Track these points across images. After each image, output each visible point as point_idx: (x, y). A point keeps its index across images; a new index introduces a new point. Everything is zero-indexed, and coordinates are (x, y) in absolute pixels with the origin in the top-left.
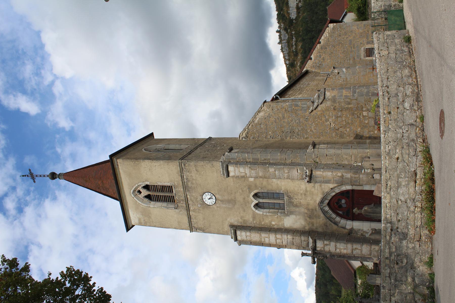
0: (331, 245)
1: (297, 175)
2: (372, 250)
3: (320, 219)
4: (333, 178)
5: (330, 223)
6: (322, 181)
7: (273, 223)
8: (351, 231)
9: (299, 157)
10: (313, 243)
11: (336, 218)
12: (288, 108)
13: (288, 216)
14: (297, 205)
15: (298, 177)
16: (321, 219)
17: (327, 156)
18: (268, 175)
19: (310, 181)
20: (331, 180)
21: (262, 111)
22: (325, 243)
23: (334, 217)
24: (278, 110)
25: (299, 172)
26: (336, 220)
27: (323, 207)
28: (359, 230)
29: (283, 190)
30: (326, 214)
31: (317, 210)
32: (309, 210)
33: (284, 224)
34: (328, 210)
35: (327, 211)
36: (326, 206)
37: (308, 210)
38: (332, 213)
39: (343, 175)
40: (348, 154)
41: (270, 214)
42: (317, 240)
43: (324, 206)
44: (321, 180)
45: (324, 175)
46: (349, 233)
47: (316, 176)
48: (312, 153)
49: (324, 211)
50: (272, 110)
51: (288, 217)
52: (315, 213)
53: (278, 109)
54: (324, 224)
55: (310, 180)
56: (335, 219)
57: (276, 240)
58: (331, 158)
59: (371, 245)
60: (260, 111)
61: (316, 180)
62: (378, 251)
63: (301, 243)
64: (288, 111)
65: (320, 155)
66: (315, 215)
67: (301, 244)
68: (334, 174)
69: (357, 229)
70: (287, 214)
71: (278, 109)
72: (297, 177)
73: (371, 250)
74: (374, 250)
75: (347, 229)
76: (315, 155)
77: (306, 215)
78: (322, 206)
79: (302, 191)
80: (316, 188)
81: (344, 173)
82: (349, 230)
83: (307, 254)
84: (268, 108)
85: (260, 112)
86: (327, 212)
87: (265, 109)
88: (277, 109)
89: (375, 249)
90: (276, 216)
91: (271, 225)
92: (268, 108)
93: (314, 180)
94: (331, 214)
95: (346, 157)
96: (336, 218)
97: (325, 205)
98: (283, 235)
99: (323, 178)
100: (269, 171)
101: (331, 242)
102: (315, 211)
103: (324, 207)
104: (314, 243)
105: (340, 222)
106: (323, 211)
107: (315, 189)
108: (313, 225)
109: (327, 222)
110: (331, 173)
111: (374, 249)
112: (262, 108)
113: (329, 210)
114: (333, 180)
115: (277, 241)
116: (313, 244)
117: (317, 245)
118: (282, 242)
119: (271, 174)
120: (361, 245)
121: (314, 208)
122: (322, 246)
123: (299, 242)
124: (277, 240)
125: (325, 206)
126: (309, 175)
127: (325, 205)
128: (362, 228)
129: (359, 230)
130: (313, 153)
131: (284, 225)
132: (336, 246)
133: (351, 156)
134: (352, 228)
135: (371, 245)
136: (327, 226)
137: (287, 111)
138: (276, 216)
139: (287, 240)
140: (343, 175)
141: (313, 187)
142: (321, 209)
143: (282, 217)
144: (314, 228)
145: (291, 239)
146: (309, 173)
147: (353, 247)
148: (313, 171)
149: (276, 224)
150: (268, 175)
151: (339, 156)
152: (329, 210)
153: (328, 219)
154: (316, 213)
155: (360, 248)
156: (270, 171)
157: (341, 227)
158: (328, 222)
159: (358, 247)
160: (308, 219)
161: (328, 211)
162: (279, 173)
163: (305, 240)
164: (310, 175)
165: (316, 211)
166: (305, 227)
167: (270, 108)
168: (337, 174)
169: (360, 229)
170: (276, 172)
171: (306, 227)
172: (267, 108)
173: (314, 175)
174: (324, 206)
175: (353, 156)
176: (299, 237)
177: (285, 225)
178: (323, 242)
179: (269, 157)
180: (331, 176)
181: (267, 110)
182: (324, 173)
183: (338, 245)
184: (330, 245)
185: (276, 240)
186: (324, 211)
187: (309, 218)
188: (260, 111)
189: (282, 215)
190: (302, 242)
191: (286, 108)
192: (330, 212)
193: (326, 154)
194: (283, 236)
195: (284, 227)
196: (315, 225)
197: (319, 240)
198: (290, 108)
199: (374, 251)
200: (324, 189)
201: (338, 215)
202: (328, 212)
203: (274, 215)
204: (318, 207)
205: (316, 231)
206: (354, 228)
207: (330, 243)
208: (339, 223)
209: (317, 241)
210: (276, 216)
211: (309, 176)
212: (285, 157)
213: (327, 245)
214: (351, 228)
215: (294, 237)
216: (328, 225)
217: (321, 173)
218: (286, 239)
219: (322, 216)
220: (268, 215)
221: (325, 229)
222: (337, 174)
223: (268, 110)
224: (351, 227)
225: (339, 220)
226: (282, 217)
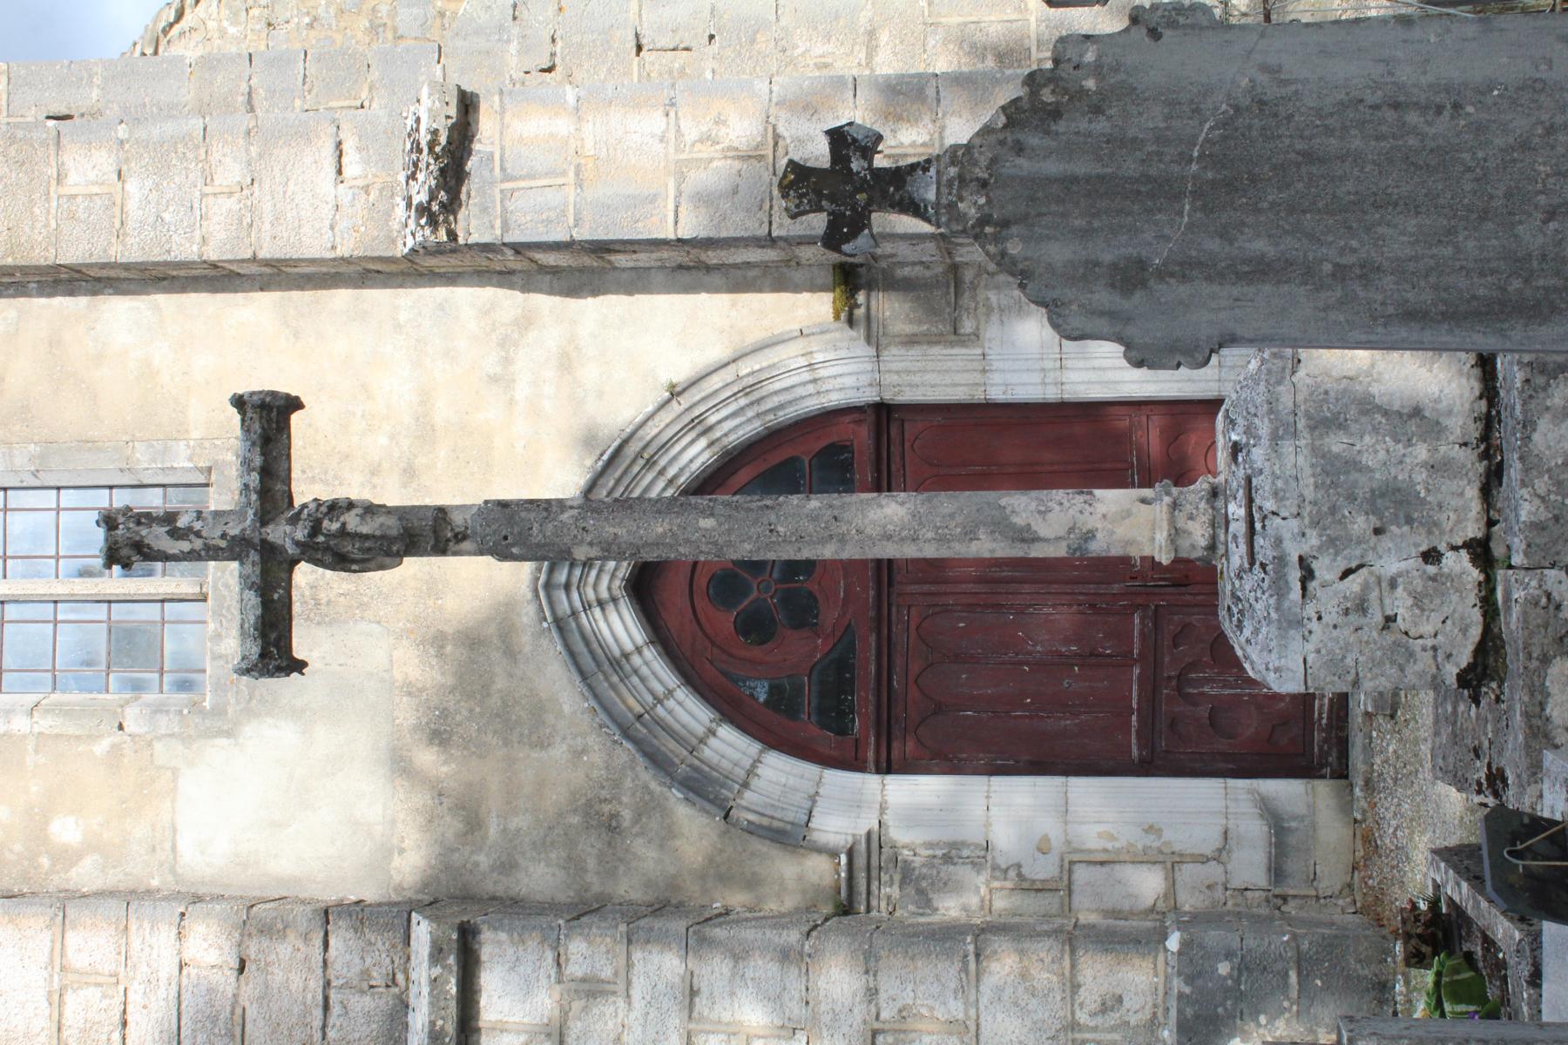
0: (636, 993)
1: (327, 211)
2: (1082, 1017)
3: (543, 744)
4: (681, 178)
5: (646, 787)
6: (564, 213)
7: (66, 831)
8: (861, 877)
9: (375, 74)
10: (437, 954)
11: (713, 733)
12: (393, 13)
13: (229, 734)
14: (318, 604)
15: (342, 225)
16: (559, 752)
17: (639, 48)
18: (47, 225)
19: (442, 205)
20: (653, 199)
21: (182, 34)
22: (579, 974)
23: (693, 725)
24: (311, 26)
25: (352, 167)
26: (707, 753)
27: (587, 607)
28: (947, 859)
29: (195, 434)
30: (613, 687)
31: (525, 640)
32: (440, 655)
33: (175, 831)
34: (629, 647)
35: (626, 656)
36: (614, 600)
37: (438, 641)
38: (669, 678)
39: (777, 138)
40: (837, 18)
41: (45, 723)
42: (486, 935)
43: (591, 595)
44: (553, 198)
45: (589, 144)
46: (844, 894)
47: (508, 165)
48: (501, 28)
49: (591, 652)
50: (269, 25)
51: (217, 751)
52: (500, 683)
53: (315, 19)
54: (589, 804)
55: (443, 196)
56: (702, 741)
57: (61, 1004)
58: (682, 70)
59: (1073, 952)
60: (165, 32)
61: (511, 206)
62: (1153, 1024)
63: (318, 1013)
64: (395, 29)
65: (576, 39)
66: (495, 701)
67: (318, 1036)
68: (691, 132)
69: (930, 845)
70: (219, 712)
71: (315, 19)
72: (332, 228)
73: (1074, 1026)
74: (1113, 1018)
75: (819, 850)
76: (524, 50)
77: (406, 714)
78: (567, 587)
79: (383, 440)
80: (522, 391)
81: (783, 115)
82: (844, 859)
83: (182, 522)
84: (236, 14)
85: (163, 42)
86: (619, 664)
87: (211, 24)
88: (307, 20)
89: (1120, 1000)
90: (101, 747)
91: (45, 861)
92: (236, 14)
93: (484, 210)
94: (659, 689)
95: (819, 49)
96: (713, 733)
97: (604, 595)
98: (133, 927)
99: (579, 184)
100: (60, 180)
101: (637, 955)
102: (496, 655)
103: (597, 612)
104: (452, 960)
105: (751, 772)
106: (580, 647)
107: (511, 402)
108: (473, 824)
109: (617, 784)
110: (655, 122)
111: (1104, 1009)
112: (187, 11)
113: (639, 650)
114: (679, 194)
115: (68, 1011)
116: (437, 971)
117: (483, 1002)
118: (117, 1018)
119: (72, 217)
120: (965, 969)
121: (492, 629)
122: (544, 1003)
123: (306, 1012)
124: (70, 998)
125: (601, 604)
126: (435, 133)
127: (604, 595)
128: (973, 834)
129: (947, 859)
130: (515, 31)
131: (174, 848)
132: (693, 993)
133: (872, 34)
134: (875, 841)
135: (1073, 952)
136: (611, 826)
137: (390, 35)
138: (92, 738)
139: (174, 988)
140: (781, 130)
141: (494, 379)
142: (559, 624)
143: (158, 746)
144: (483, 860)
145: (217, 978)
146: (433, 116)
147: (872, 993)
148: (483, 107)
149: (91, 845)
150: (47, 225)
151: (753, 41)
152: (639, 650)
153: (626, 733)
154: (511, 676)
155: (956, 1009)
156: (73, 178)
157: (753, 830)
158: (628, 783)
159: (936, 989)
160: (427, 758)
161: (636, 660)
162: (154, 196)
163: (365, 974)
164: (443, 140)
165: (511, 653)
166: (387, 851)
167: (251, 12)
168: (719, 122)
169: (955, 845)
170: (132, 186)
171: (402, 851)
172: (225, 12)
173: (492, 154)
174: (591, 595)
175: (884, 37)
176: (306, 938)
177: (182, 846)
178: (550, 956)
179: (95, 93)
180: (658, 147)
181: (223, 33)
182: (588, 128)
183: (714, 970)
184: (629, 983)
185: (57, 999)
186: (591, 652)
187: (431, 742)
188: (165, 32)
189: (164, 723)
190: (336, 1010)
191: (384, 9)
192: (656, 669)
193: (632, 37)
194: (136, 944)
195: (173, 871)
196: (493, 830)
197: (510, 932)
198: (415, 11)
199: (1113, 1029)
200: (601, 395)
201: (731, 708)
202: (636, 672)
203: (78, 737)
204: (527, 614)
205: (500, 890)
206: (899, 834)
207: (629, 965)
208: (745, 785)
209: (486, 952)
210: (101, 747)
211: (432, 145)
212: (244, 87)
213: (592, 989)
214: (863, 832)
215: (252, 950)
216: (627, 815)
217: (563, 126)
218: (163, 975)
219: (566, 708)
220: (25, 737)
221: (591, 863)
222: (719, 122)
223: (232, 30)
224: (869, 822)
225: (747, 763)
226: (158, 746)
